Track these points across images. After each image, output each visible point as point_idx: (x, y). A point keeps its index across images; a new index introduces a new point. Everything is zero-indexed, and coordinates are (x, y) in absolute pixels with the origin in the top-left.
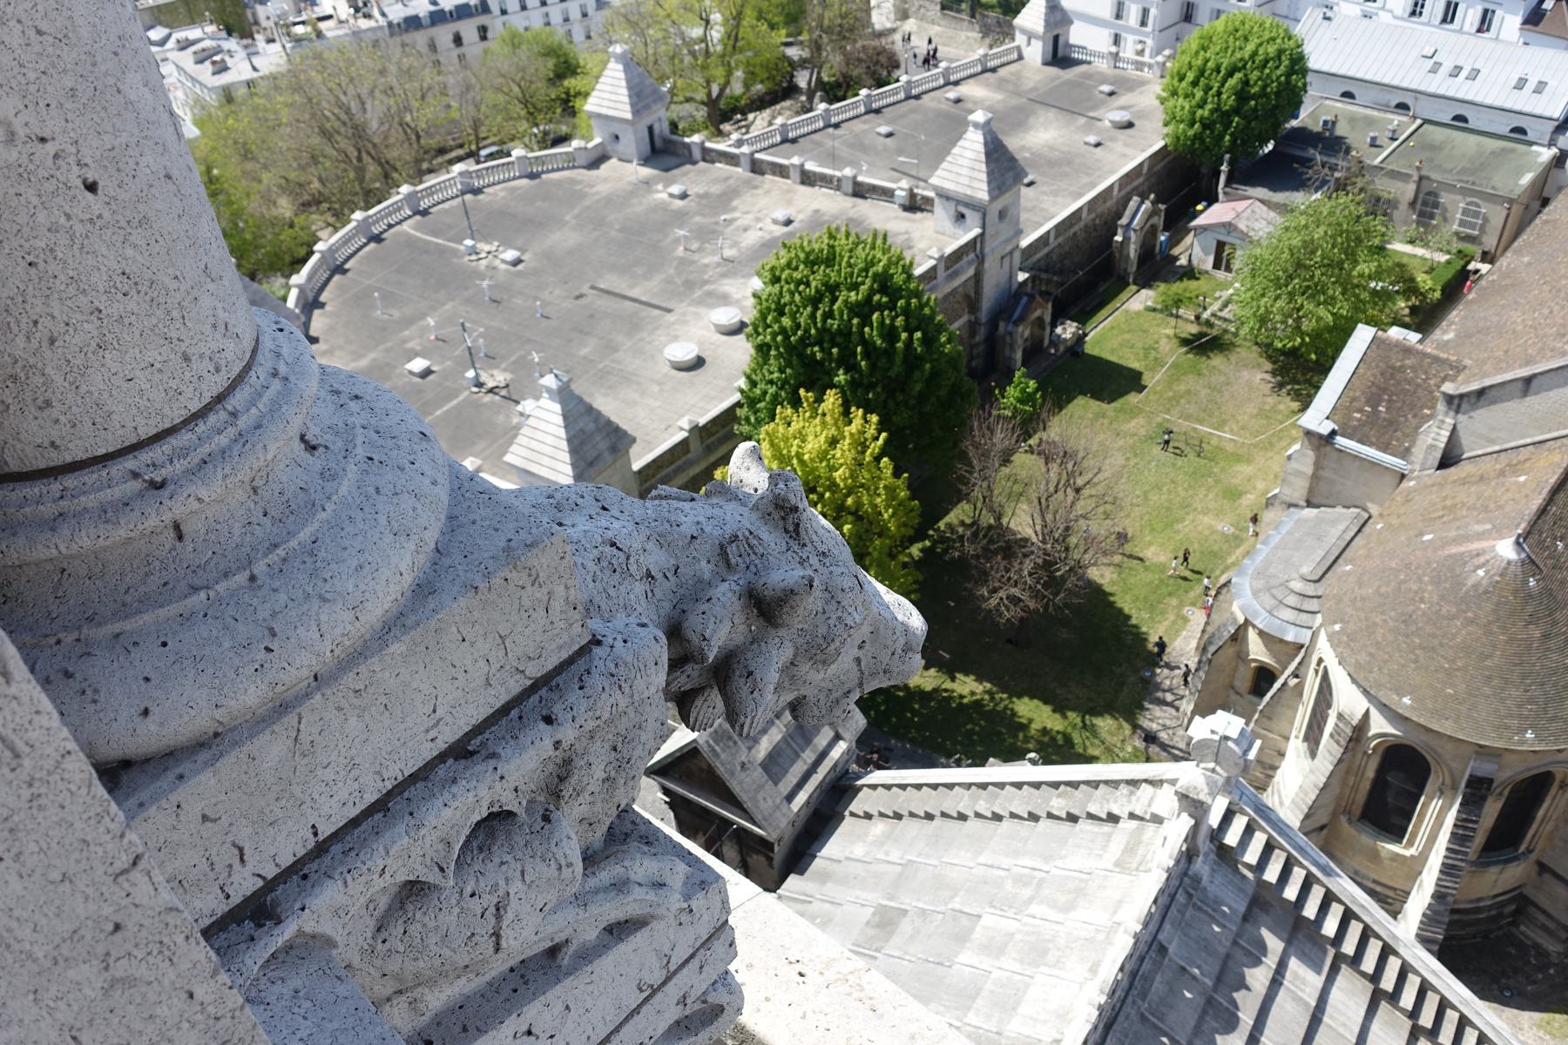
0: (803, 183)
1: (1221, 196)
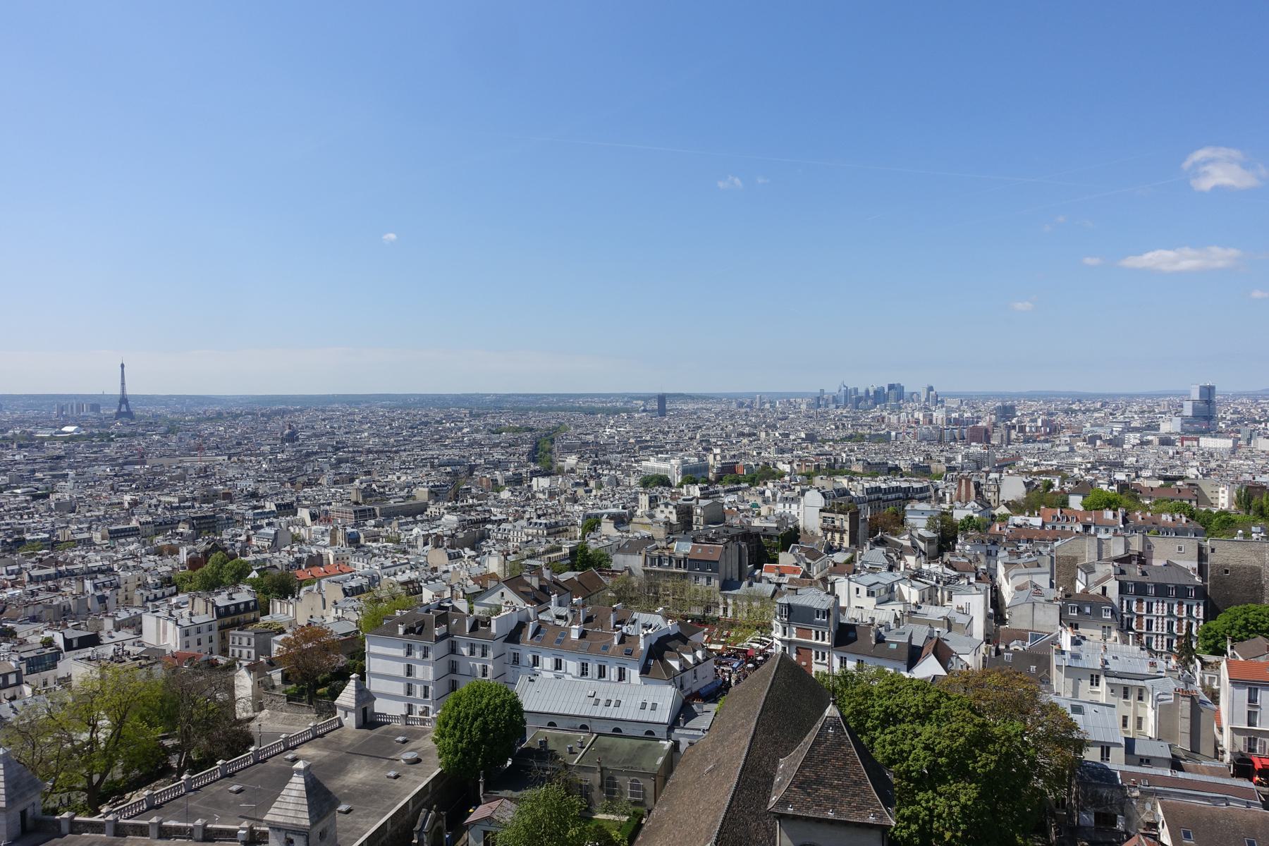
0: (160, 837)
1: (482, 799)
